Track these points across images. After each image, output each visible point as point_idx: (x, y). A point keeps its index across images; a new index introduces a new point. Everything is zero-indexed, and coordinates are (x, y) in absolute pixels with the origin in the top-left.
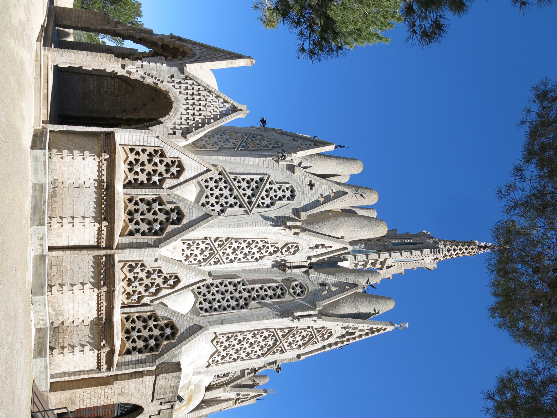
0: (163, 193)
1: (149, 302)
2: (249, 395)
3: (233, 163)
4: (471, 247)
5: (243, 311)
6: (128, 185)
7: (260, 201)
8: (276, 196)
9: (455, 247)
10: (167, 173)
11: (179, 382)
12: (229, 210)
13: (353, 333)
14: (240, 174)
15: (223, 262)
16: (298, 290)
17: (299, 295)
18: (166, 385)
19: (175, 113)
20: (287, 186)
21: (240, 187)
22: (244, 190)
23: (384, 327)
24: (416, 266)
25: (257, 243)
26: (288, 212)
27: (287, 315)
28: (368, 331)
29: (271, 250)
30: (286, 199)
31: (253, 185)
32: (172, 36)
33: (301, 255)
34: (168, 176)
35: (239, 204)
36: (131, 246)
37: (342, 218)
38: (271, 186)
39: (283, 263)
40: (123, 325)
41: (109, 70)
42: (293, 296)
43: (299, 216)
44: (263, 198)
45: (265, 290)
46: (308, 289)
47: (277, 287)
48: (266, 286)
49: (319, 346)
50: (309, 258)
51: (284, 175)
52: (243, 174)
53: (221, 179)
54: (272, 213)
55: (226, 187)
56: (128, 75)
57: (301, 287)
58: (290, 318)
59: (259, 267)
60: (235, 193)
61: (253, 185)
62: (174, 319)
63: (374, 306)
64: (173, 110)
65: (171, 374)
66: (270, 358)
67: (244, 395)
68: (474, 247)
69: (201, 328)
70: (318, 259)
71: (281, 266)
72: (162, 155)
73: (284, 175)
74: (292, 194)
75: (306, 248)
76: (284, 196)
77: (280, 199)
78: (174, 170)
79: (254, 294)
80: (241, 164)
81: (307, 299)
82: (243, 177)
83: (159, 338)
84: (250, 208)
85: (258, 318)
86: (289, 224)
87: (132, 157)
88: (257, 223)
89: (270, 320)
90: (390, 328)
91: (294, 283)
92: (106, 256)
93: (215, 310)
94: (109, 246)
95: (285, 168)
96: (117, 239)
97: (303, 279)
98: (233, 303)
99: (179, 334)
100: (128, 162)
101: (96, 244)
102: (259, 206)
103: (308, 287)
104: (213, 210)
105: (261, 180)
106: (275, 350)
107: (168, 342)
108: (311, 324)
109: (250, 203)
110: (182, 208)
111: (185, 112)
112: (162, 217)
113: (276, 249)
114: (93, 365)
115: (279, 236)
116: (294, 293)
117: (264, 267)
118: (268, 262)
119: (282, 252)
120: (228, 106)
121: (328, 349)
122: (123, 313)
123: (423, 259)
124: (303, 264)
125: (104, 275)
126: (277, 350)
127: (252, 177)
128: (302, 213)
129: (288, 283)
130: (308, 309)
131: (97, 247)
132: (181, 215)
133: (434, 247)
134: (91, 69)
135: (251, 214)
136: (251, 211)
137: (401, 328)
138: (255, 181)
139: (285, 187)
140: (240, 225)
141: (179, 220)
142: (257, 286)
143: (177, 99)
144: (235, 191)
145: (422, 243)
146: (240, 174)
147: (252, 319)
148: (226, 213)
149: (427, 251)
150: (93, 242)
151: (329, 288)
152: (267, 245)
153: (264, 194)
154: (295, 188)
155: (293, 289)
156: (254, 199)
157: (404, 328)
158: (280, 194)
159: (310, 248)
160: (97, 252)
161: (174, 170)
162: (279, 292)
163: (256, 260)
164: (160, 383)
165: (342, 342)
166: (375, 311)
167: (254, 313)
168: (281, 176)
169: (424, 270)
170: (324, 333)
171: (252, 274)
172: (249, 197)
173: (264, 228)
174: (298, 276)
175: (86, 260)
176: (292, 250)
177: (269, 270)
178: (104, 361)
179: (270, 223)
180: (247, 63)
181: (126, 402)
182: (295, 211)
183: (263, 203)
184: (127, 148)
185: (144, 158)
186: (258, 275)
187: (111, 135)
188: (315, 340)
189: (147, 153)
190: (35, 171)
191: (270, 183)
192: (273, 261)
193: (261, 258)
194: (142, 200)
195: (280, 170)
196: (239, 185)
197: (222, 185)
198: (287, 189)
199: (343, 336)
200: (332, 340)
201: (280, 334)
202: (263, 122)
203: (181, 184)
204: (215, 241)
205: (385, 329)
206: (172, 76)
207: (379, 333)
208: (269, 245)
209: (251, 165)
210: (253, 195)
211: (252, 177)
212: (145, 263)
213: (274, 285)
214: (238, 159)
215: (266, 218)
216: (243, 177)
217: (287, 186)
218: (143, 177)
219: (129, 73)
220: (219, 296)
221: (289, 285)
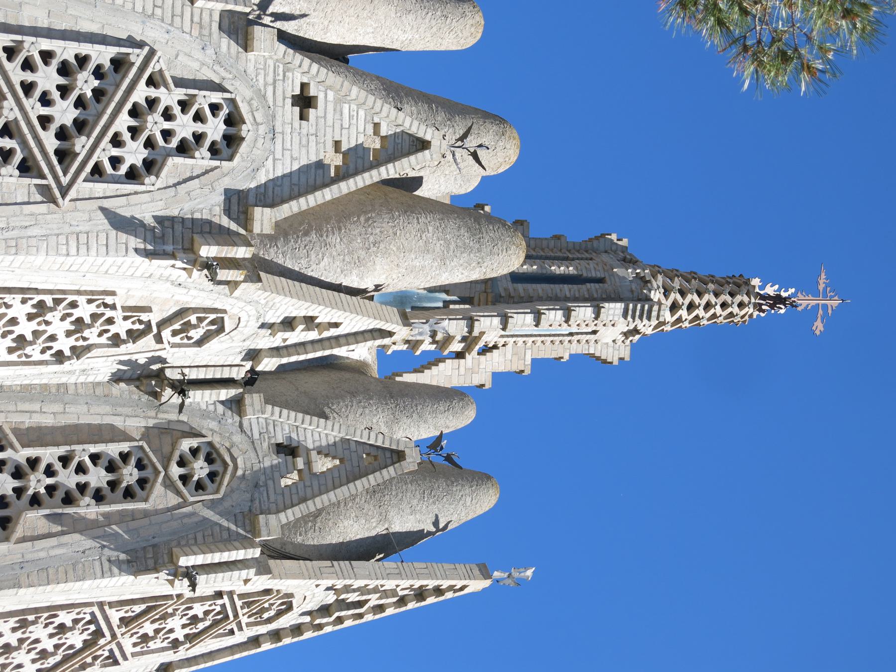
7: (104, 153)
9: (695, 298)
13: (360, 604)
14: (36, 32)
16: (200, 469)
17: (200, 486)
20: (216, 97)
21: (28, 88)
22: (45, 100)
23: (459, 584)
24: (565, 351)
25: (73, 305)
26: (205, 203)
27: (151, 563)
28: (406, 592)
29: (121, 327)
30: (204, 151)
31: (86, 83)
33: (225, 345)
35: (18, 157)
37: (386, 217)
38: (153, 92)
39: (155, 367)
42: (178, 493)
43: (245, 220)
44: (117, 141)
45: (81, 469)
46: (236, 468)
47: (125, 457)
48: (83, 452)
49: (240, 637)
50: (253, 355)
51: (210, 51)
52: (50, 33)
54: (147, 203)
57: (209, 460)
59: (64, 380)
61: (86, 83)
63: (435, 509)
68: (746, 299)
70: (285, 361)
71: (147, 378)
73: (210, 51)
74: (232, 130)
77: (183, 149)
79: (37, 483)
81: (227, 504)
82: (46, 44)
84: (65, 180)
85: (46, 574)
86: (208, 251)
88: (83, 238)
89: (88, 583)
90: (477, 585)
91: (186, 445)
95: (215, 26)
97: (220, 431)
102: (97, 172)
103: (234, 459)
105: (119, 64)
109: (64, 156)
116: (184, 479)
117: (82, 379)
118: (101, 365)
121: (266, 646)
123: (594, 332)
124: (226, 374)
127: (85, 49)
128: (258, 212)
129: (167, 440)
130: (229, 541)
133: (635, 297)
135: (65, 203)
137: (509, 582)
138: (91, 66)
139: (204, 99)
142: (49, 455)
145: (601, 281)
146: (36, 32)
147: (24, 579)
149: (613, 310)
151: (308, 463)
152: (109, 313)
153: (124, 121)
154: (244, 109)
155: (181, 463)
156: (81, 145)
157: (519, 583)
158: (184, 126)
159: (263, 326)
162: (130, 475)
163: (60, 357)
166: (436, 523)
167: (29, 557)
168: (198, 55)
171: (36, 406)
172: (62, 134)
173: (110, 260)
174: (205, 414)
177: (99, 391)
179: (134, 242)
182: (234, 200)
186: (57, 407)
192: (121, 363)
193: (78, 352)
195: (195, 33)
196: (29, 77)
198: (215, 108)
199: (325, 610)
201: (115, 616)
205: (462, 588)
208: (118, 314)
210: (80, 126)
213: (113, 450)
215: (122, 224)
216: (46, 44)
217: (216, 97)
221: (167, 449)
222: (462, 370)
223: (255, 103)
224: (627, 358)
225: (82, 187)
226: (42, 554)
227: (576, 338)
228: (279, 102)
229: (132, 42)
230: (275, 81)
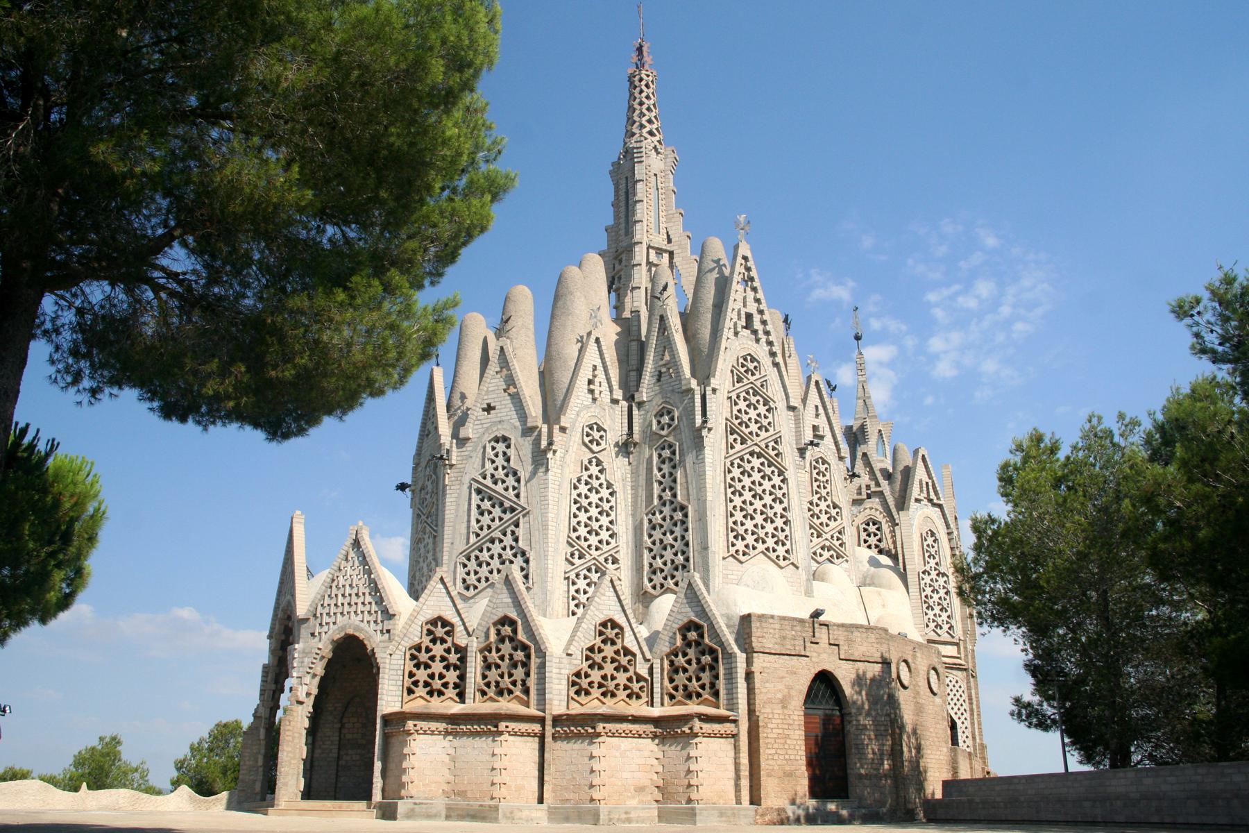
0: (474, 645)
1: (648, 665)
2: (921, 481)
3: (453, 538)
4: (637, 83)
5: (690, 515)
6: (461, 696)
8: (504, 468)
10: (446, 642)
11: (772, 617)
12: (521, 544)
13: (749, 317)
14: (468, 527)
16: (666, 419)
19: (361, 630)
20: (489, 449)
21: (489, 527)
28: (748, 289)
29: (594, 470)
30: (508, 451)
31: (487, 504)
32: (270, 637)
34: (449, 639)
36: (542, 692)
38: (489, 477)
40: (680, 703)
41: (306, 724)
43: (533, 429)
44: (506, 489)
49: (772, 373)
53: (477, 558)
55: (489, 549)
56: (312, 698)
57: (662, 415)
58: (704, 433)
64: (357, 634)
65: (754, 630)
66: (790, 458)
67: (921, 491)
68: (637, 78)
69: (690, 584)
72: (418, 648)
75: (595, 409)
76: (505, 454)
77: (508, 460)
78: (440, 632)
80: (454, 527)
82: (473, 522)
83: (700, 648)
86: (544, 443)
92: (554, 726)
93: (687, 560)
94: (542, 721)
96: (533, 711)
98: (678, 531)
99: (696, 620)
100: (428, 697)
101: (537, 739)
102: (518, 496)
105: (479, 492)
106: (773, 453)
107: (706, 635)
108: (722, 396)
109: (513, 510)
110: (496, 618)
111: (360, 617)
112: (506, 648)
114: (726, 746)
115: (567, 458)
120: (352, 554)
122: (662, 704)
125: (580, 727)
126: (774, 449)
127: (474, 507)
128: (529, 425)
131: (542, 738)
132: (505, 621)
134: (305, 748)
136: (524, 509)
140: (545, 527)
141: (512, 623)
142: (656, 489)
143: (343, 628)
144: (493, 535)
146: (468, 527)
148: (525, 548)
149: (639, 171)
150: (534, 744)
152: (585, 477)
153: (499, 487)
156: (507, 504)
158: (500, 461)
160: (548, 739)
161: (440, 632)
165: (767, 333)
169: (678, 169)
170: (743, 370)
172: (504, 512)
175: (559, 751)
176: (596, 435)
178: (716, 727)
183: (514, 488)
184: (406, 697)
185: (422, 675)
187: (387, 719)
189: (414, 670)
190: (429, 816)
194: (484, 677)
197: (485, 556)
198: (493, 448)
199: (755, 332)
200: (761, 351)
201: (738, 447)
202: (402, 487)
203: (462, 620)
204: (573, 564)
205: (745, 258)
206: (313, 635)
207: (753, 267)
209: (457, 510)
210: (501, 504)
211: (474, 507)
212: (575, 671)
214: (448, 531)
216: (473, 522)
217: (489, 449)
218: (452, 676)
219: (308, 694)
220: (669, 554)
225: (522, 501)
227: (660, 185)
229: (470, 487)
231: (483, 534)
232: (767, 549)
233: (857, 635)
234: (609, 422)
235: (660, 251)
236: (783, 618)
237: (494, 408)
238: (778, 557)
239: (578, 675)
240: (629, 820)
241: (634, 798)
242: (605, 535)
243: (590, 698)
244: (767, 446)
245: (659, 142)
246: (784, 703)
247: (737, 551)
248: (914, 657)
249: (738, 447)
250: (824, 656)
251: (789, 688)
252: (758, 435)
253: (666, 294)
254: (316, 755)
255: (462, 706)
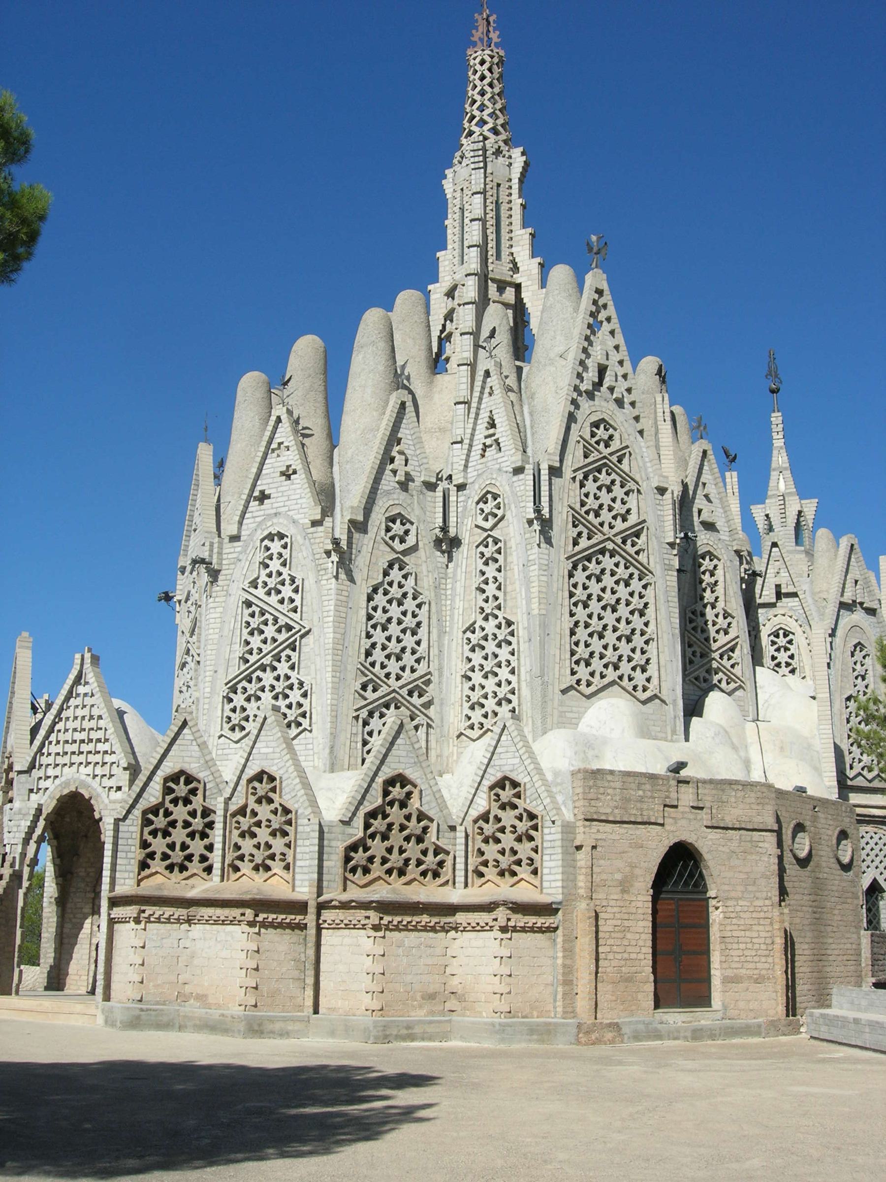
11: (612, 772)
15: (422, 677)
18: (617, 798)
60: (267, 660)
62: (487, 783)
72: (155, 810)
84: (297, 627)
87: (157, 865)
100: (167, 873)
104: (255, 716)
113: (396, 566)
119: (405, 553)
143: (67, 784)
153: (274, 599)
154: (266, 533)
156: (283, 620)
164: (609, 811)
168: (243, 562)
172: (279, 631)
178: (531, 920)
180: (27, 648)
181: (650, 879)
185: (159, 844)
188: (614, 459)
191: (256, 588)
195: (232, 566)
222: (529, 283)
223: (264, 527)
224: (521, 149)
226: (524, 602)
228: (262, 513)
230: (253, 517)
231: (252, 659)
232: (621, 678)
233: (731, 795)
234: (417, 511)
235: (502, 286)
236: (628, 774)
237: (268, 497)
238: (635, 688)
239: (353, 848)
240: (412, 1038)
241: (421, 1007)
242: (408, 659)
243: (369, 877)
244: (624, 542)
245: (506, 142)
246: (625, 886)
247: (578, 682)
248: (815, 819)
249: (584, 543)
250: (683, 822)
251: (633, 866)
252: (611, 527)
253: (494, 342)
254: (66, 930)
255: (208, 885)
